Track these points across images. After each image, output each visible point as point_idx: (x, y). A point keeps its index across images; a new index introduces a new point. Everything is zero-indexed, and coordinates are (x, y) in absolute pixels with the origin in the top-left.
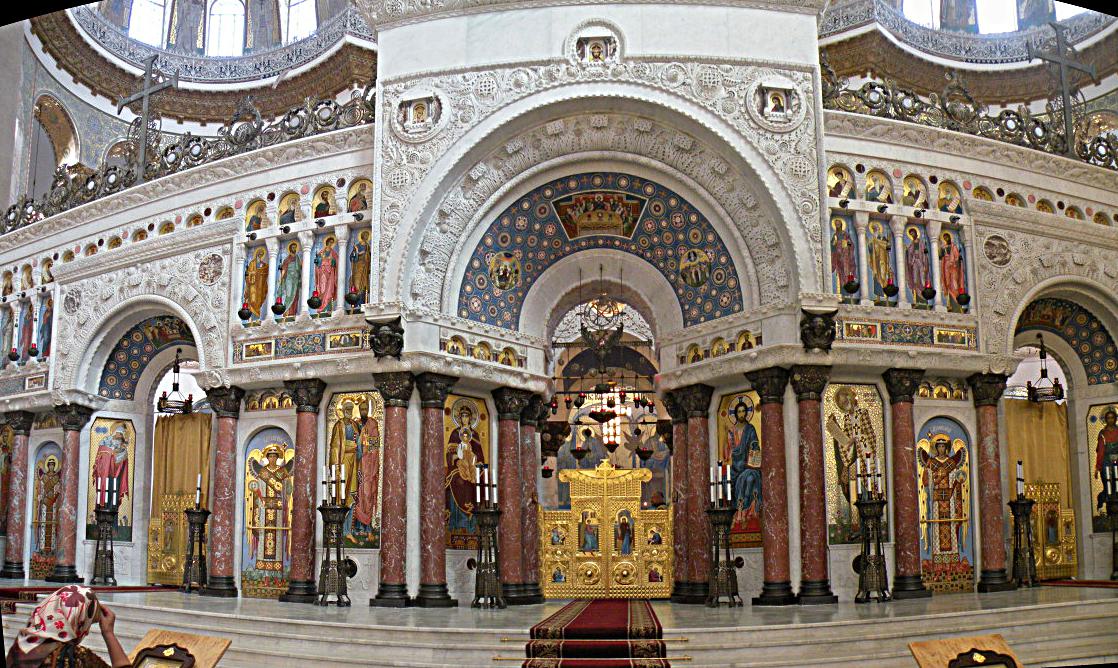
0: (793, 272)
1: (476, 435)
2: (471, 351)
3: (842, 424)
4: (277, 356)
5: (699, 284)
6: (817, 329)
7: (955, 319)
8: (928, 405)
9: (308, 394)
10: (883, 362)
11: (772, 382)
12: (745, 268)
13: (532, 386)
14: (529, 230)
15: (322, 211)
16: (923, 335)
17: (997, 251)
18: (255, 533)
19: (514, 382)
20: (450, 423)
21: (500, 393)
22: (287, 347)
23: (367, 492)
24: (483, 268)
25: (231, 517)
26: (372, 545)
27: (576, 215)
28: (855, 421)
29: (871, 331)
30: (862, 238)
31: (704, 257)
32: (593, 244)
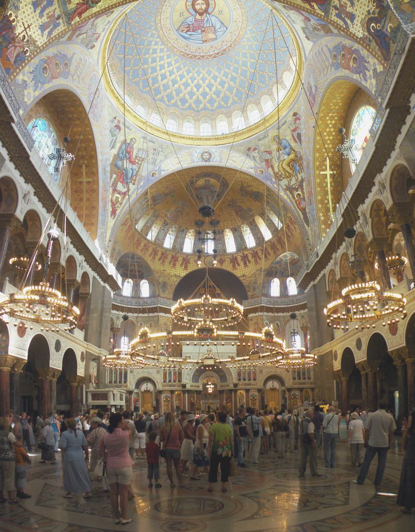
0: (232, 377)
6: (235, 385)
7: (254, 382)
9: (172, 392)
11: (231, 391)
12: (227, 377)
16: (250, 384)
17: (261, 372)
21: (197, 391)
22: (170, 386)
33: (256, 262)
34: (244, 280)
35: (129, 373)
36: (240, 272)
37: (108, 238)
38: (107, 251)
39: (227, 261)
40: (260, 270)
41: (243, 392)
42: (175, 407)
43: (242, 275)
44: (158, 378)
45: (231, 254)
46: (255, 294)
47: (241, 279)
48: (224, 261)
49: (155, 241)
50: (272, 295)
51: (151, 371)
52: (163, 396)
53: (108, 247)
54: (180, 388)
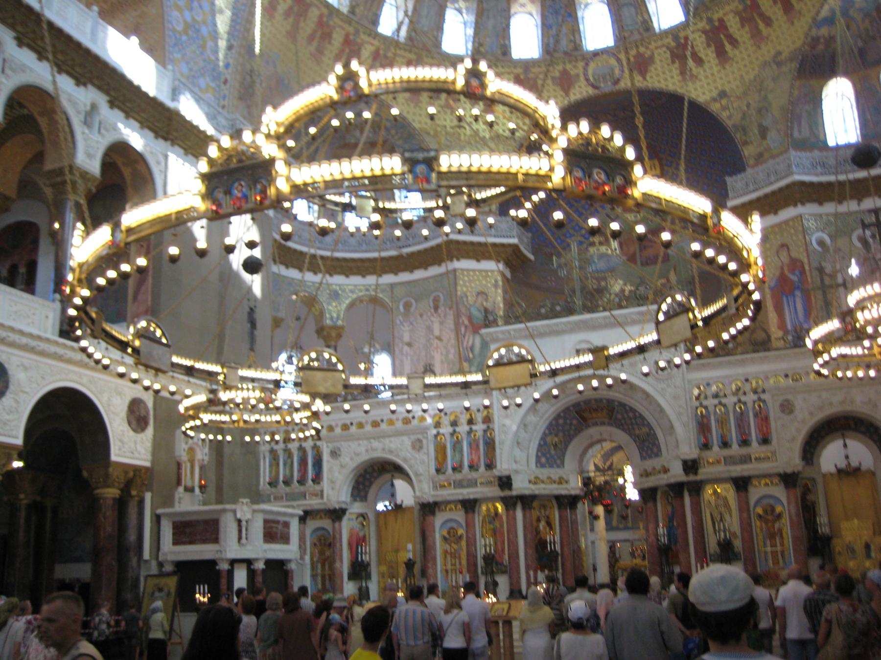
1: (548, 517)
2: (543, 482)
3: (713, 504)
4: (455, 487)
5: (644, 441)
8: (755, 493)
9: (469, 505)
10: (726, 475)
13: (573, 493)
14: (565, 423)
15: (470, 422)
18: (447, 571)
19: (564, 492)
20: (535, 513)
21: (558, 498)
22: (459, 484)
23: (500, 548)
24: (545, 443)
25: (435, 563)
26: (504, 572)
27: (586, 415)
28: (721, 502)
29: (719, 462)
30: (712, 418)
31: (645, 430)
32: (596, 424)
33: (756, 35)
34: (724, 108)
35: (326, 457)
36: (704, 86)
37: (222, 44)
38: (226, 82)
39: (661, 57)
40: (777, 61)
41: (726, 491)
42: (480, 562)
43: (715, 94)
44: (420, 464)
45: (673, 32)
46: (768, 149)
47: (715, 108)
48: (651, 59)
49: (409, 38)
50: (831, 143)
51: (394, 443)
52: (439, 519)
53: (227, 66)
54: (495, 491)
